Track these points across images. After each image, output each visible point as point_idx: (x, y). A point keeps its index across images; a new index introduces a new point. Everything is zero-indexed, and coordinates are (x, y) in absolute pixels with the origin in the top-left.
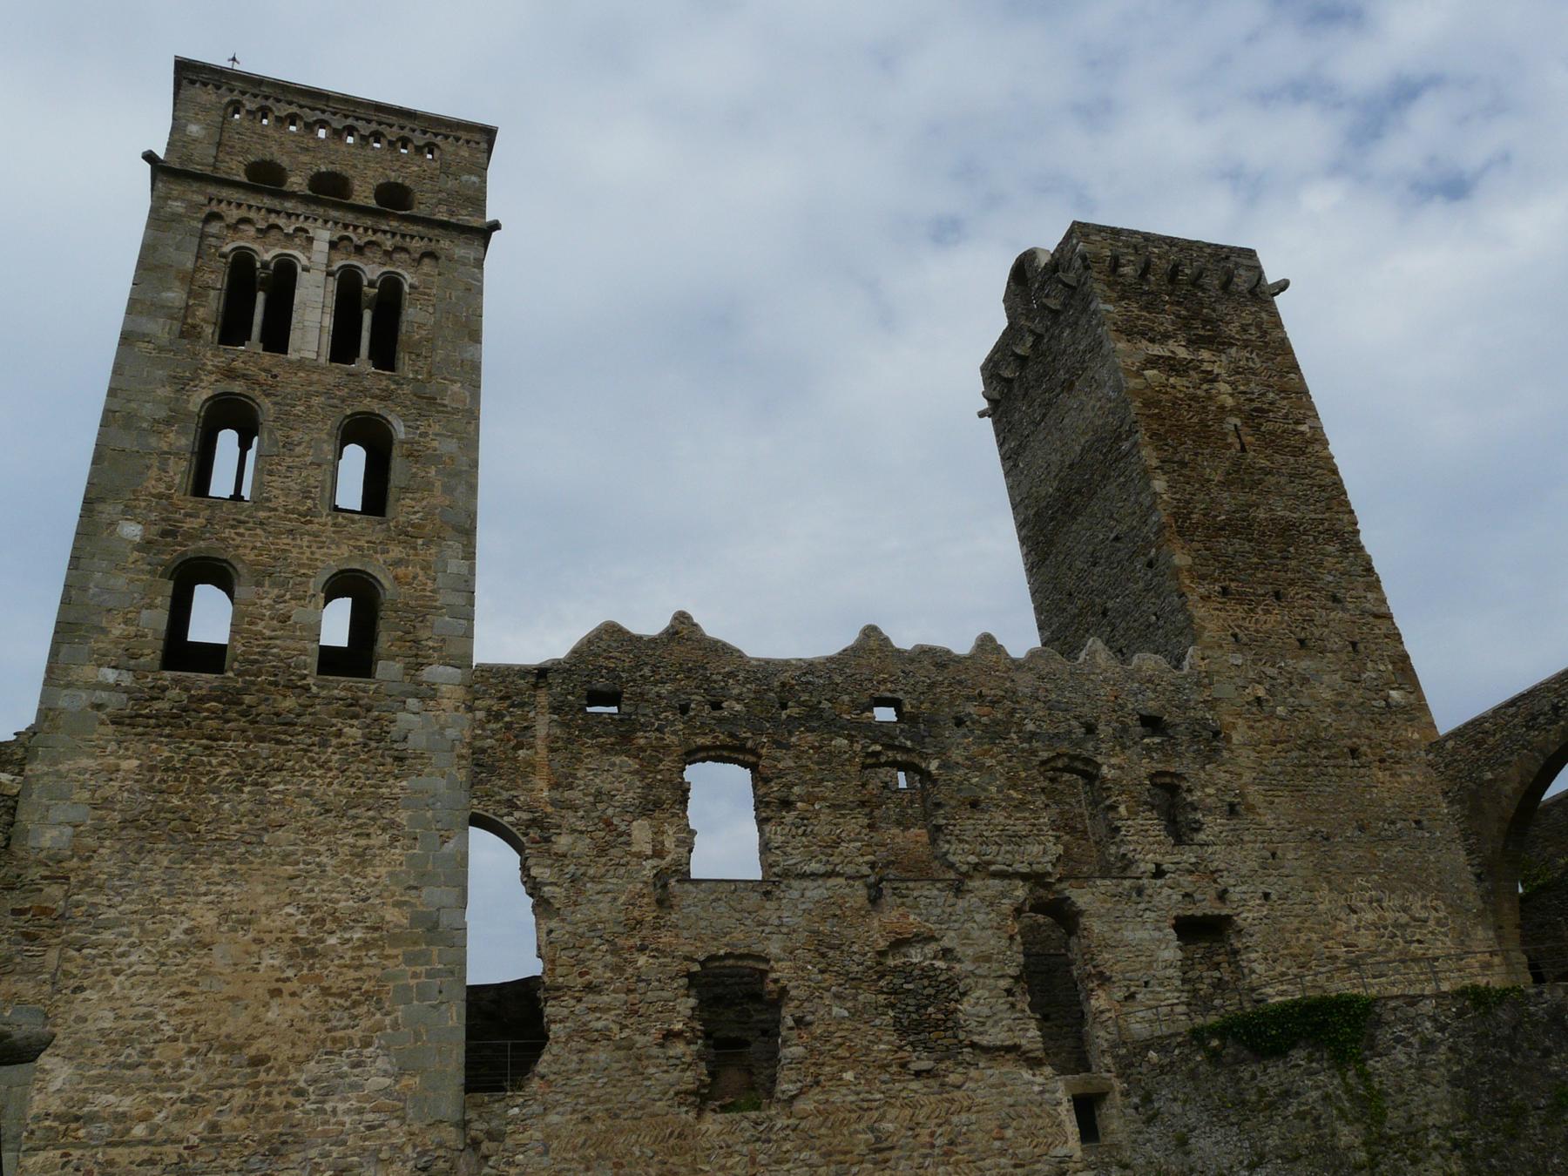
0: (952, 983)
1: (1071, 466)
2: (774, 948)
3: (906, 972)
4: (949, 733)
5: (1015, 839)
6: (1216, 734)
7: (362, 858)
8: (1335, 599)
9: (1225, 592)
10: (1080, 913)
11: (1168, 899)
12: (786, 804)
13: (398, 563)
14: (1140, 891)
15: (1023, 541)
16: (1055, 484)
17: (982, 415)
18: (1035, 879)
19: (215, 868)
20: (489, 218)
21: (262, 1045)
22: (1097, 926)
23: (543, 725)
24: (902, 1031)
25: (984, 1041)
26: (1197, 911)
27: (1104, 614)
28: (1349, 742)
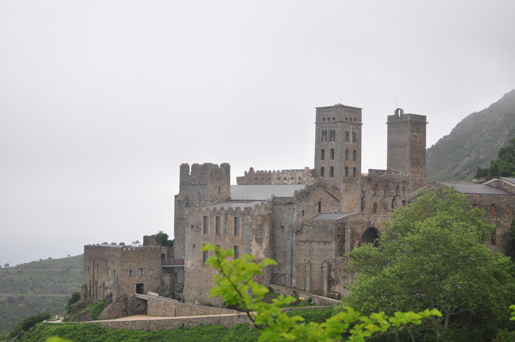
0: (388, 205)
1: (399, 142)
2: (378, 202)
3: (385, 204)
4: (390, 183)
5: (393, 193)
6: (408, 182)
7: (356, 193)
8: (421, 167)
9: (413, 166)
10: (396, 200)
11: (402, 199)
12: (379, 189)
13: (357, 166)
14: (400, 198)
15: (388, 145)
16: (396, 142)
17: (386, 123)
18: (394, 196)
19: (349, 194)
20: (362, 123)
21: (351, 208)
22: (397, 201)
23: (366, 182)
24: (385, 209)
25: (389, 210)
26: (404, 200)
27: (398, 162)
28: (418, 184)
